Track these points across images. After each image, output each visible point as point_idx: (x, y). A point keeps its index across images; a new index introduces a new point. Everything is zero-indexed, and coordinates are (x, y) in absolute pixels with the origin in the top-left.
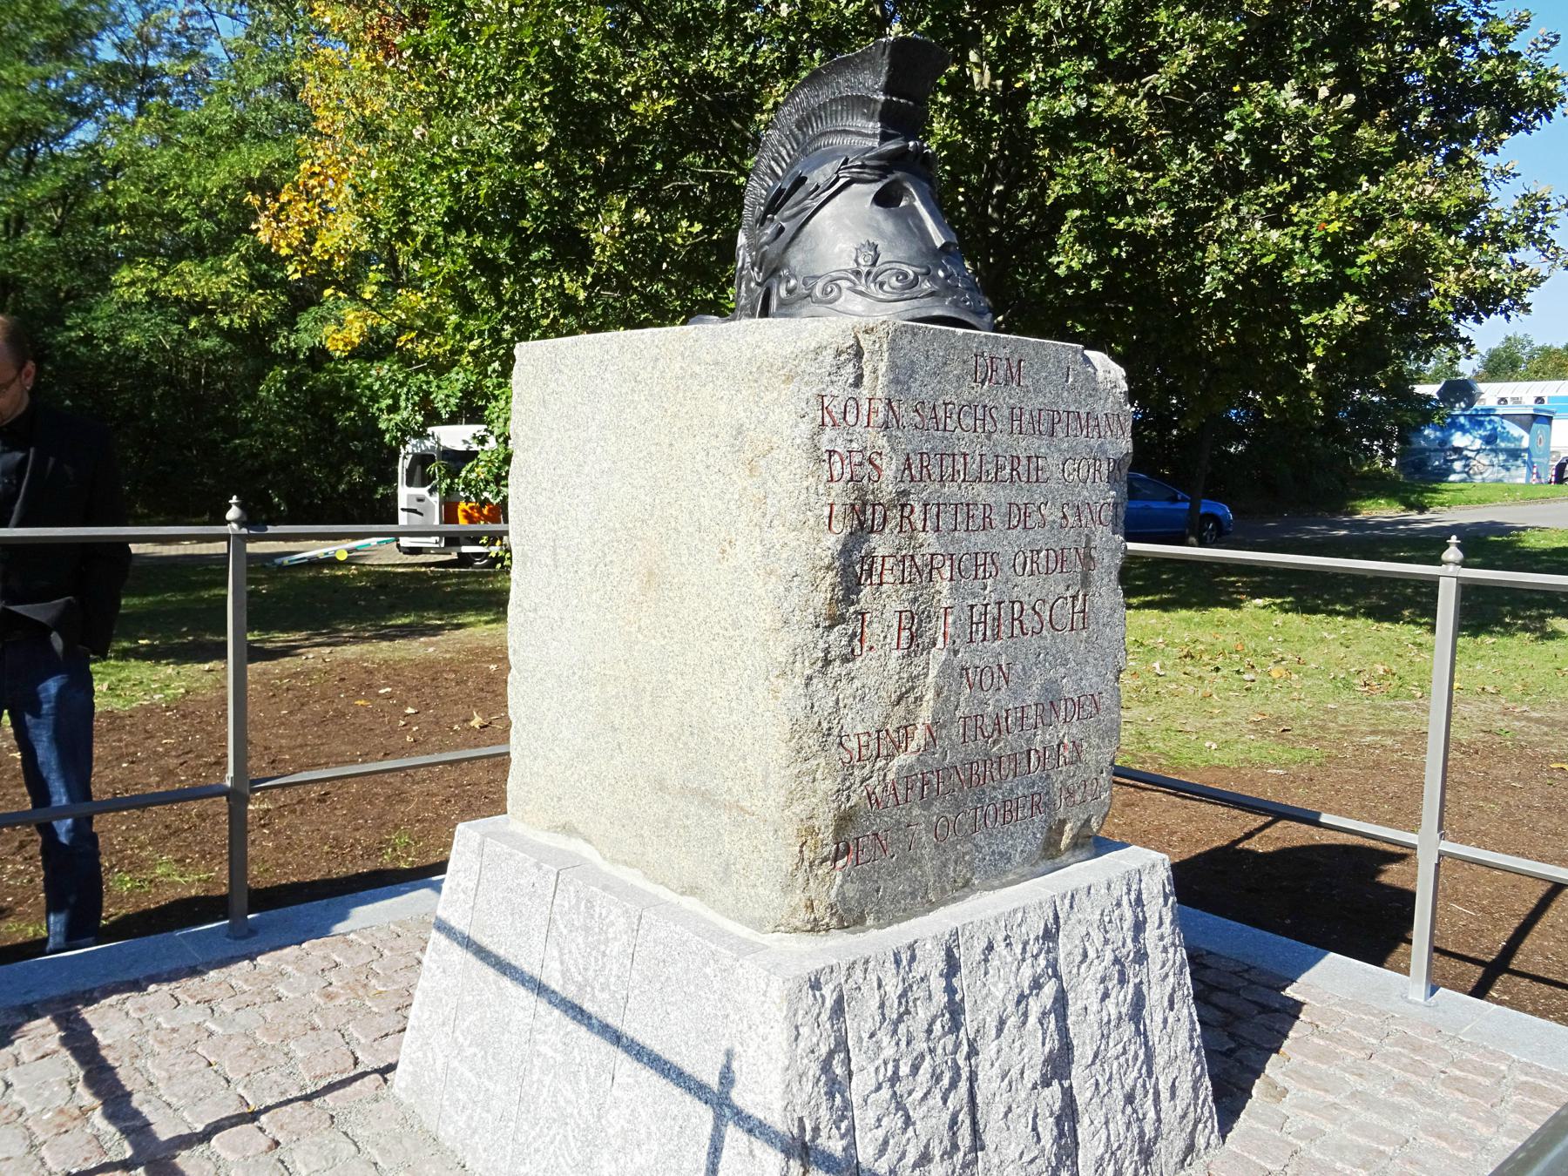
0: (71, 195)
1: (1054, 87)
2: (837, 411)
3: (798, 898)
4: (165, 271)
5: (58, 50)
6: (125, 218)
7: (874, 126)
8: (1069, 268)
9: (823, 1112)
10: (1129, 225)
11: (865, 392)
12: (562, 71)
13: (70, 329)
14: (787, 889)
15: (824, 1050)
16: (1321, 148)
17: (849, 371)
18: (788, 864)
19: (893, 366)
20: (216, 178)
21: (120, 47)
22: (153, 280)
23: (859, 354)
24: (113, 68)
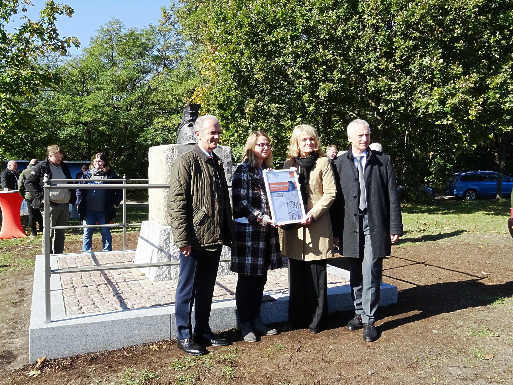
0: (143, 97)
1: (369, 61)
2: (170, 156)
3: (166, 221)
4: (167, 119)
5: (141, 55)
6: (156, 103)
7: (189, 116)
8: (384, 110)
9: (164, 246)
10: (391, 97)
11: (174, 154)
12: (237, 67)
13: (141, 137)
14: (165, 219)
15: (165, 238)
16: (437, 74)
17: (172, 151)
18: (165, 216)
19: (179, 150)
20: (181, 89)
21: (159, 50)
22: (164, 122)
23: (173, 149)
24: (157, 57)
